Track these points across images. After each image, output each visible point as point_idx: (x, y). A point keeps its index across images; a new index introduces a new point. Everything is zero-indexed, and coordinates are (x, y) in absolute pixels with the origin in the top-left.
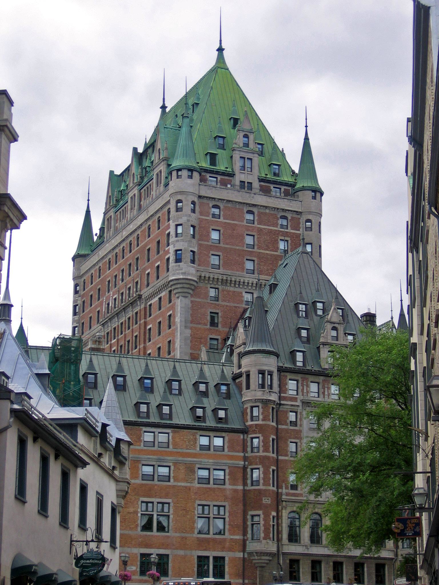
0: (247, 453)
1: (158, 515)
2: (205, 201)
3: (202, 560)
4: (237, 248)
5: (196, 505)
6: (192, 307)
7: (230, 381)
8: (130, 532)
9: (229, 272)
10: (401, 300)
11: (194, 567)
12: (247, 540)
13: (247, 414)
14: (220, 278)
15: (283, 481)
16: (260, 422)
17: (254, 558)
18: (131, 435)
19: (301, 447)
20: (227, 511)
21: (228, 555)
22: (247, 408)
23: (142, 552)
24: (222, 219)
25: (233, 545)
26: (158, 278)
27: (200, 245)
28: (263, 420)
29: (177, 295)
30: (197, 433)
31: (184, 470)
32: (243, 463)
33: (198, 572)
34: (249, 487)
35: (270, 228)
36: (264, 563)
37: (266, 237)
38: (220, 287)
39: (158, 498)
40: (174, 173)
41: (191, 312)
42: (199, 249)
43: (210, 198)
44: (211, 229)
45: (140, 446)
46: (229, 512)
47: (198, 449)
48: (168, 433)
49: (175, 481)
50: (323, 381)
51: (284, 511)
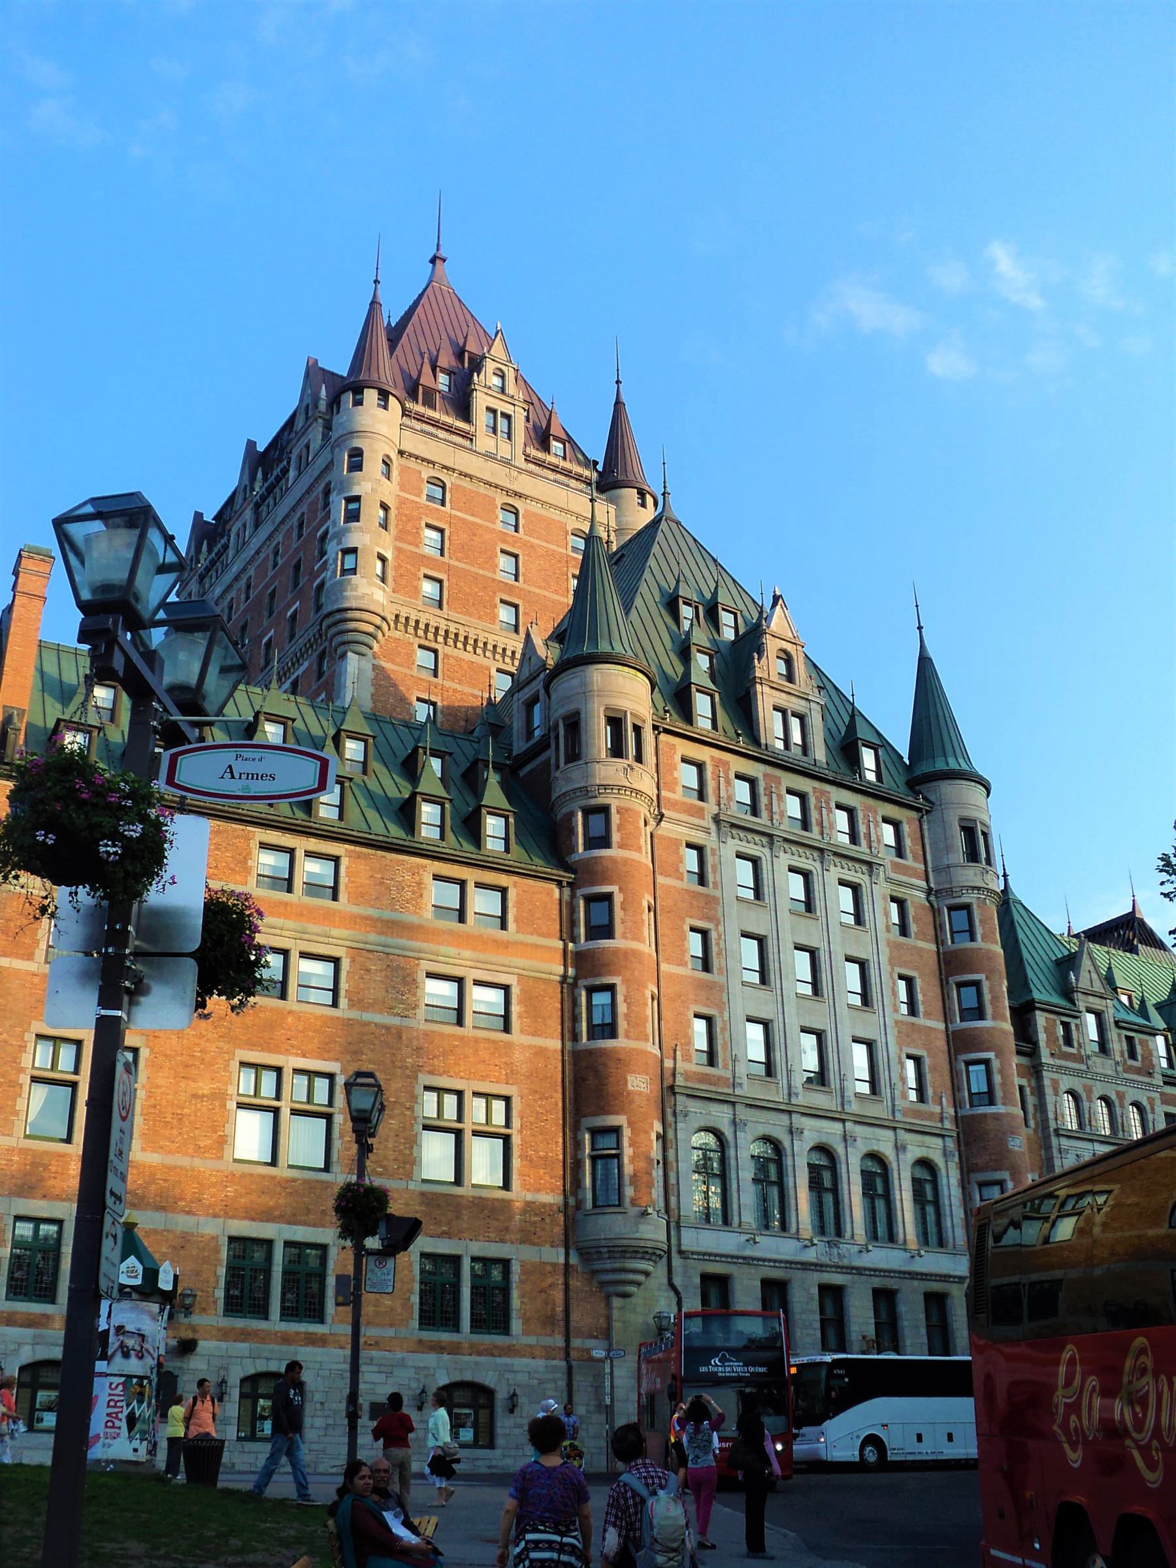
2: (412, 464)
4: (481, 572)
8: (198, 1163)
10: (920, 628)
11: (411, 1291)
13: (572, 831)
18: (217, 849)
19: (718, 944)
21: (520, 1255)
22: (572, 814)
23: (235, 1233)
25: (535, 1223)
26: (292, 636)
27: (398, 550)
31: (383, 973)
32: (561, 970)
33: (421, 1310)
37: (542, 562)
39: (297, 1055)
40: (349, 398)
41: (372, 690)
42: (396, 558)
43: (423, 460)
48: (336, 860)
49: (352, 1004)
50: (765, 776)
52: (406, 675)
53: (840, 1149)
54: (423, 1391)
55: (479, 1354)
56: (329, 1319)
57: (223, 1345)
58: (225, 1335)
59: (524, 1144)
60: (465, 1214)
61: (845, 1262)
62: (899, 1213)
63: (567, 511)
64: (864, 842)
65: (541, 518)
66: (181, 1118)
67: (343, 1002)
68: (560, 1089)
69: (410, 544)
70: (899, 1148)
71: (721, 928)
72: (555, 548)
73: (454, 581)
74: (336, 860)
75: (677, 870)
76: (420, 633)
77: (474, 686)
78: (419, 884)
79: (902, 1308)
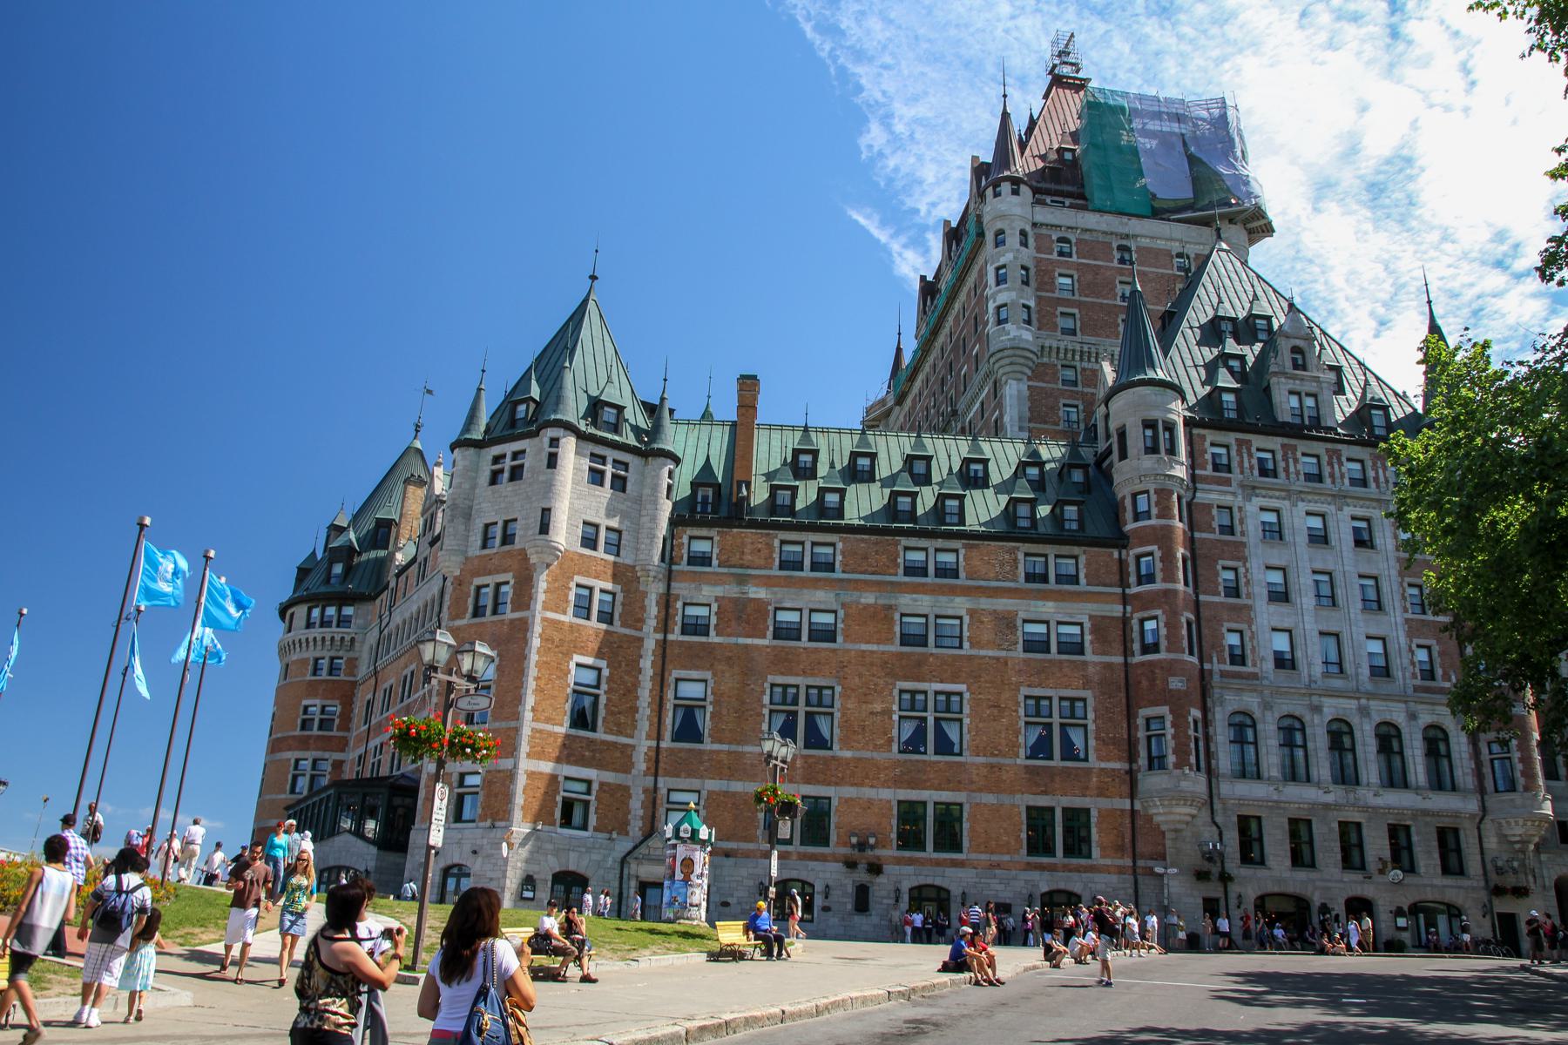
0: (1129, 587)
2: (1044, 231)
3: (1039, 820)
5: (1021, 698)
6: (1031, 395)
8: (875, 755)
9: (1092, 340)
11: (1020, 831)
14: (1078, 347)
15: (1213, 647)
16: (1153, 522)
17: (1155, 811)
20: (1090, 709)
21: (1095, 805)
22: (1124, 498)
23: (901, 798)
27: (1039, 299)
28: (1158, 517)
29: (1004, 379)
30: (1018, 548)
32: (1120, 608)
34: (1138, 658)
35: (1161, 271)
36: (1179, 822)
38: (1078, 364)
40: (989, 192)
41: (1029, 404)
45: (896, 575)
46: (1095, 711)
49: (972, 646)
50: (1283, 446)
51: (1218, 709)
53: (1355, 721)
54: (1030, 896)
55: (1070, 871)
56: (965, 850)
58: (899, 861)
59: (1098, 730)
60: (1057, 779)
64: (1373, 485)
65: (1148, 250)
66: (863, 728)
67: (966, 645)
68: (1123, 690)
70: (1413, 716)
71: (1248, 565)
75: (1210, 525)
76: (1062, 355)
78: (1016, 560)
79: (1415, 838)
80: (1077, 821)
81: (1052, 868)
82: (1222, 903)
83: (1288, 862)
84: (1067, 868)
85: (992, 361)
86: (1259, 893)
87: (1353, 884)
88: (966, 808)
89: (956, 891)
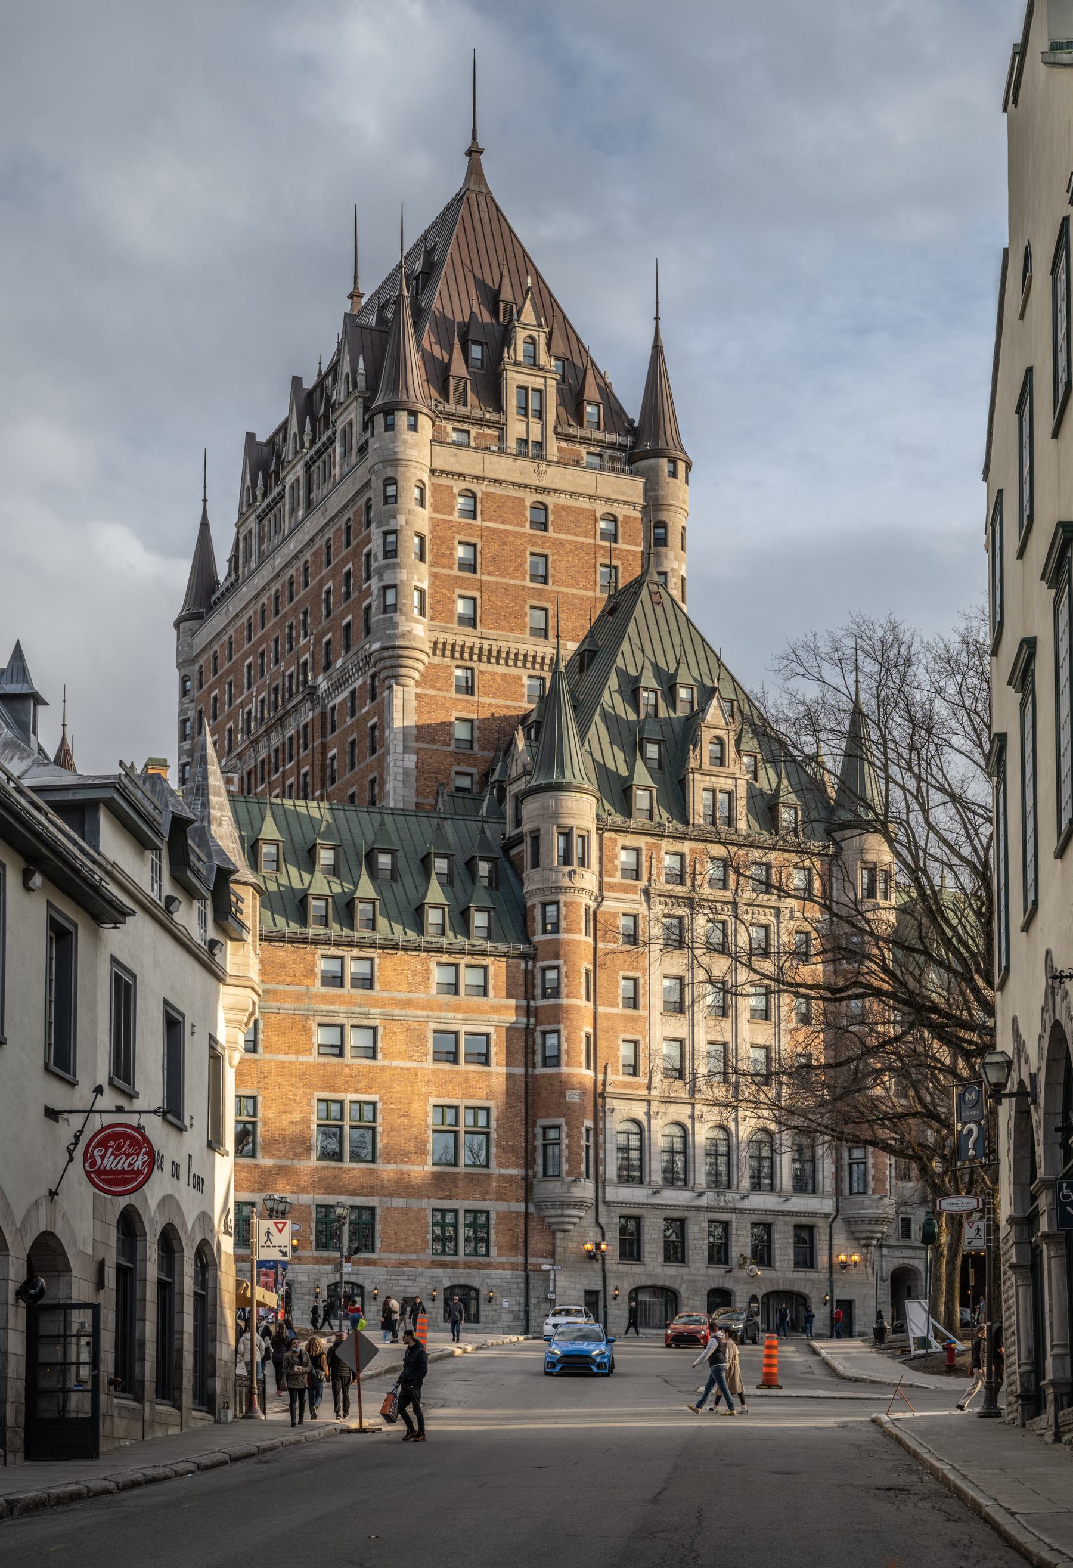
0: (534, 999)
1: (351, 1127)
4: (512, 582)
5: (430, 1108)
7: (497, 853)
9: (493, 633)
11: (427, 1232)
12: (534, 1176)
13: (534, 918)
19: (644, 987)
21: (496, 1208)
22: (534, 906)
24: (479, 522)
27: (434, 576)
34: (540, 1071)
42: (432, 584)
44: (456, 542)
46: (497, 1121)
47: (434, 991)
48: (371, 960)
49: (385, 1056)
52: (445, 698)
55: (469, 1268)
56: (377, 1250)
57: (316, 1267)
61: (730, 1205)
62: (778, 1170)
63: (596, 497)
68: (523, 1100)
69: (444, 567)
72: (584, 540)
73: (485, 597)
74: (371, 960)
77: (507, 698)
78: (427, 970)
79: (776, 1236)
80: (479, 1223)
81: (454, 1265)
82: (602, 1295)
83: (661, 1259)
84: (468, 1266)
85: (380, 666)
86: (634, 1286)
87: (716, 1276)
88: (378, 1212)
89: (368, 1287)
